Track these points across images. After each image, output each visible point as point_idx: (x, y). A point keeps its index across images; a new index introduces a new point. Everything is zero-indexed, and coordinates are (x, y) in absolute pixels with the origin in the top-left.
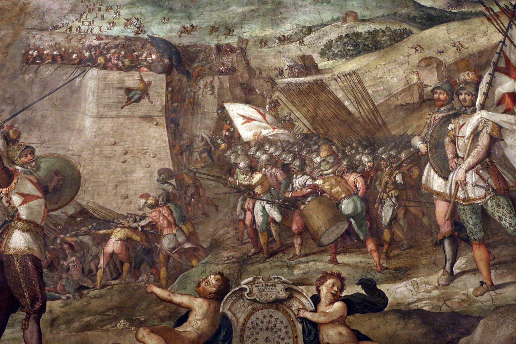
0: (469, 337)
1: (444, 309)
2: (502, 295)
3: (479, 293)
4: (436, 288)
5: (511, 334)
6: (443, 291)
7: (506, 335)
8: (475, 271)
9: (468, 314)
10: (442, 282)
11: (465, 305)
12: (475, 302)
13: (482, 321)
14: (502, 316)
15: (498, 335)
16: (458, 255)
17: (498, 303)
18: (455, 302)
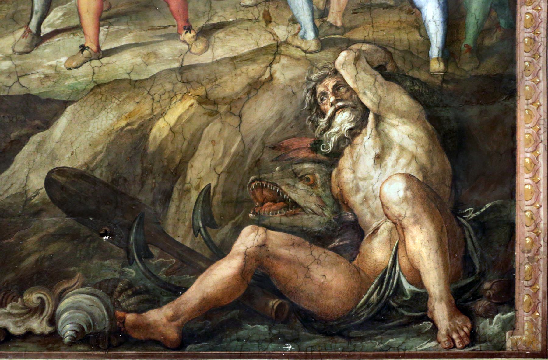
0: (47, 132)
1: (17, 90)
2: (110, 65)
3: (74, 64)
4: (8, 57)
5: (111, 125)
6: (17, 62)
7: (103, 127)
8: (77, 28)
9: (52, 97)
10: (20, 49)
11: (50, 83)
12: (67, 77)
13: (70, 108)
14: (103, 98)
15: (90, 129)
16: (53, 4)
17: (102, 78)
18: (35, 79)
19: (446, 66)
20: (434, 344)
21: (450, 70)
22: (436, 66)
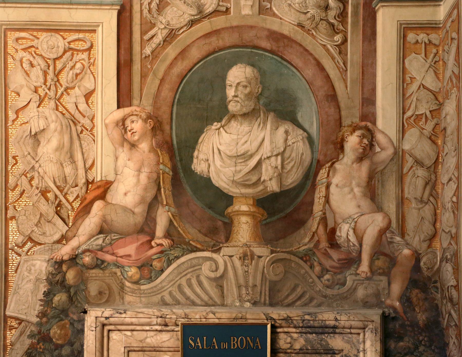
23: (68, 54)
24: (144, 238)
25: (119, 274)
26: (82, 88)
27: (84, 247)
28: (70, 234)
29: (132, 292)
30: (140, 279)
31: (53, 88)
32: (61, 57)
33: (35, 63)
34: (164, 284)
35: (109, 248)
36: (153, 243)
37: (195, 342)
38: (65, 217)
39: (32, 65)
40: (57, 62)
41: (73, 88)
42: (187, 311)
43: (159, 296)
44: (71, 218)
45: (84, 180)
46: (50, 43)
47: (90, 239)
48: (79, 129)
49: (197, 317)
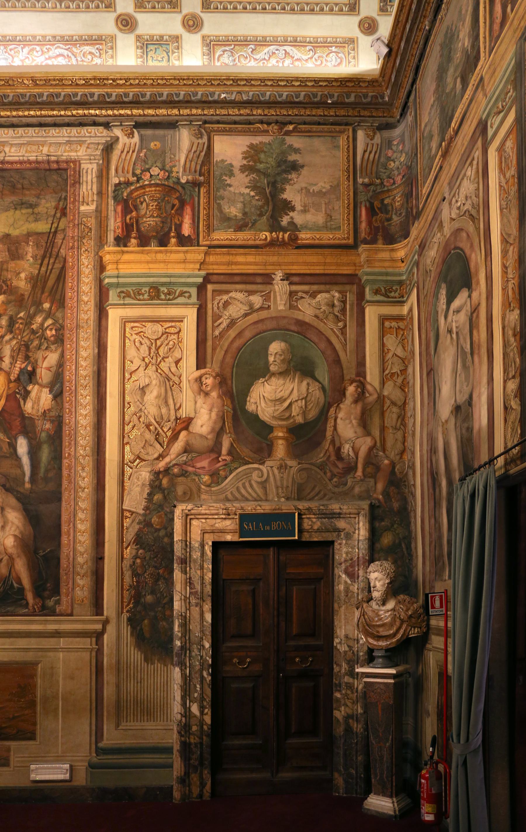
19: (32, 486)
20: (27, 610)
21: (33, 488)
22: (28, 486)
23: (165, 336)
24: (214, 456)
25: (197, 480)
26: (173, 357)
27: (174, 462)
28: (165, 453)
29: (206, 493)
30: (211, 483)
31: (155, 358)
32: (160, 338)
33: (143, 342)
34: (227, 486)
35: (190, 463)
36: (220, 459)
37: (248, 525)
38: (162, 442)
39: (141, 344)
40: (158, 341)
41: (168, 357)
42: (243, 505)
43: (224, 495)
44: (165, 443)
45: (174, 417)
46: (153, 329)
47: (177, 457)
48: (171, 384)
49: (249, 508)
